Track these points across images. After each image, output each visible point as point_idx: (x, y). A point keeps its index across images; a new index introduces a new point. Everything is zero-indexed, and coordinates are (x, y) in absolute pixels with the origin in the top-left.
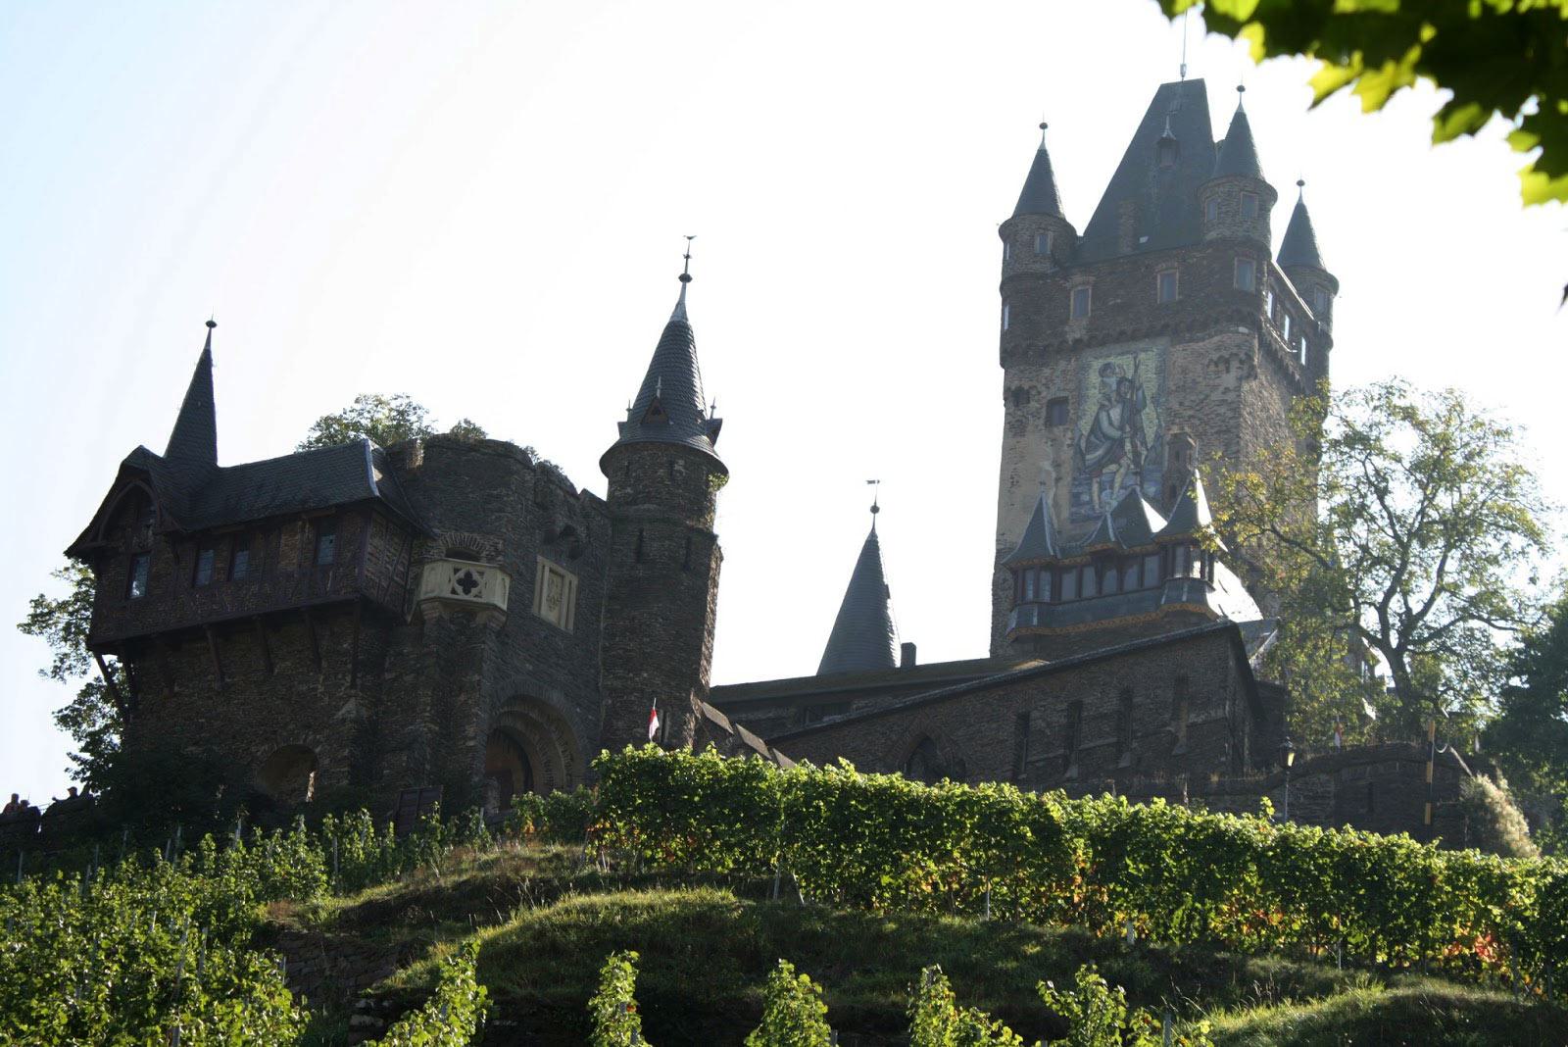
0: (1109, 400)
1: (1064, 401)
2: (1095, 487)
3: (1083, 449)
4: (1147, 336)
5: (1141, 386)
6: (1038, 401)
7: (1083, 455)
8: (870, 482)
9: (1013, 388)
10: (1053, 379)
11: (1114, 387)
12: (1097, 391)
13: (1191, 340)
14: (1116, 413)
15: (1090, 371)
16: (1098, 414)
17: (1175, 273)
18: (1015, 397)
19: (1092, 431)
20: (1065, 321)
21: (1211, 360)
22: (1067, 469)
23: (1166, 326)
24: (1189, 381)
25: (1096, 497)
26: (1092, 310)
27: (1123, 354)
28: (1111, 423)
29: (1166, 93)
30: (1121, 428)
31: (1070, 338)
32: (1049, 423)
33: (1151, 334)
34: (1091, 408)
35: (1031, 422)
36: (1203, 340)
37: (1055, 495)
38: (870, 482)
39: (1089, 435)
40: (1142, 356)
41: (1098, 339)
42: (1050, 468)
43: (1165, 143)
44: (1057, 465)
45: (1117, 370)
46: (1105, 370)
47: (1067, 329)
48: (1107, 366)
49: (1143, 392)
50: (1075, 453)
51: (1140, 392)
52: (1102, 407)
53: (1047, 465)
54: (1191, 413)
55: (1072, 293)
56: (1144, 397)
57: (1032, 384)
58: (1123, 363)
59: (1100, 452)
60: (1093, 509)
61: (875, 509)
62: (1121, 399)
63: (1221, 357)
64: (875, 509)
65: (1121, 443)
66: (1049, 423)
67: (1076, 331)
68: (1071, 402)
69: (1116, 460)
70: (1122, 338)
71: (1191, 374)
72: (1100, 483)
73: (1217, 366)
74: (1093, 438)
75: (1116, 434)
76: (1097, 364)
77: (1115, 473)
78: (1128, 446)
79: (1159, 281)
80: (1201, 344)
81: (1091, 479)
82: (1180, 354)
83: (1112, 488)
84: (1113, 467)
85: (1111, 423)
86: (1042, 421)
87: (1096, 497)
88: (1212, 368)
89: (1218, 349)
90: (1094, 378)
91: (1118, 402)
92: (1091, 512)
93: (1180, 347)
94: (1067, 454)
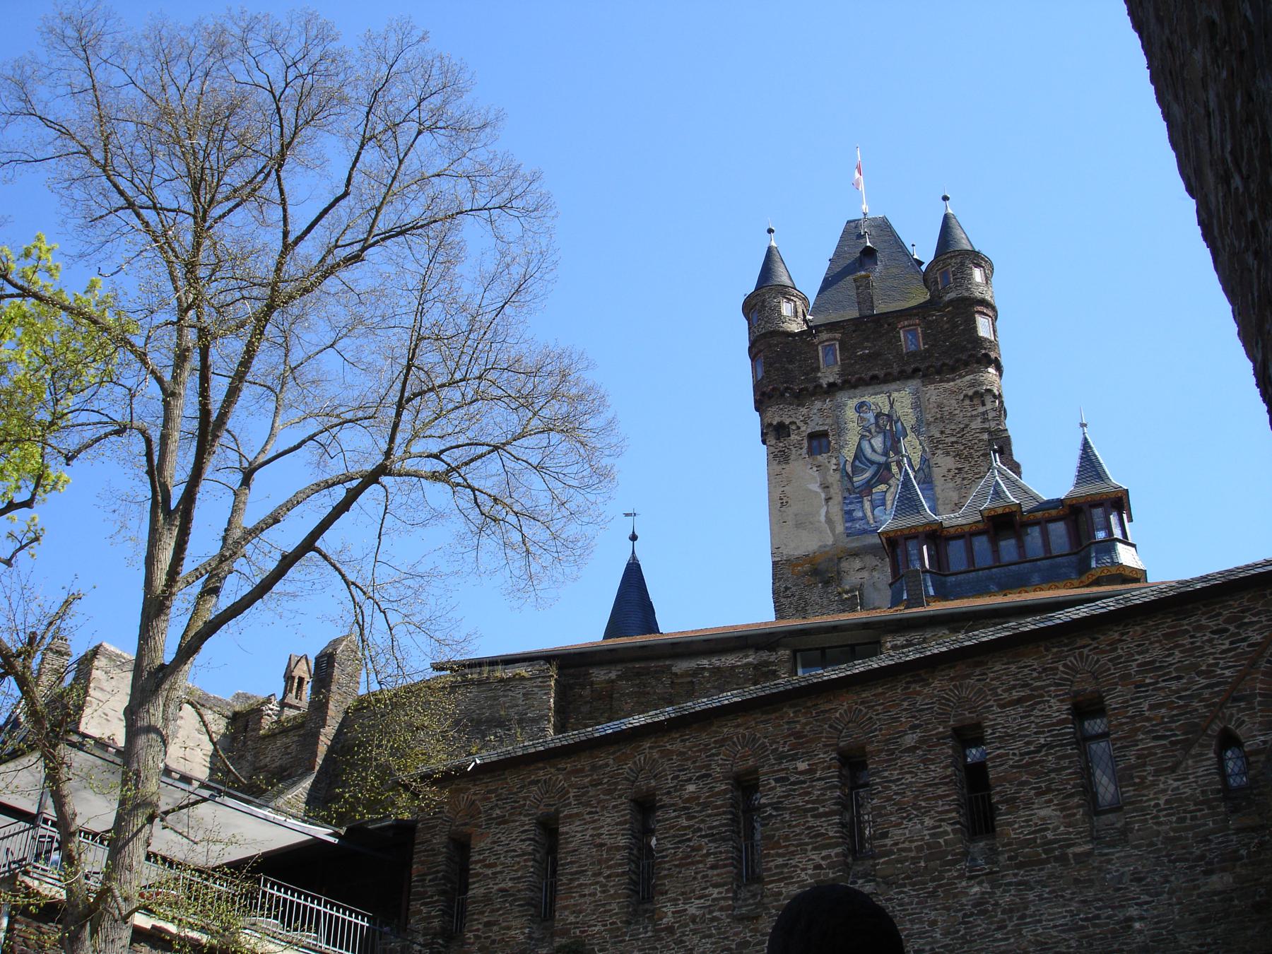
0: (870, 431)
1: (824, 434)
2: (867, 505)
3: (850, 473)
4: (895, 379)
5: (899, 419)
6: (798, 434)
7: (850, 479)
8: (627, 515)
9: (775, 423)
10: (812, 416)
11: (873, 420)
12: (855, 424)
13: (941, 381)
14: (878, 442)
15: (847, 408)
16: (859, 443)
17: (916, 329)
18: (774, 433)
19: (856, 457)
20: (818, 369)
21: (966, 396)
22: (836, 491)
23: (916, 370)
24: (946, 413)
25: (869, 514)
26: (841, 360)
27: (876, 394)
28: (874, 450)
29: (853, 230)
30: (886, 454)
31: (824, 382)
32: (812, 452)
33: (904, 376)
34: (852, 438)
35: (794, 452)
36: (953, 380)
37: (827, 512)
38: (627, 515)
39: (854, 461)
40: (895, 395)
41: (850, 382)
42: (819, 490)
43: (869, 253)
44: (826, 487)
45: (873, 407)
46: (860, 407)
47: (819, 374)
48: (862, 404)
49: (902, 424)
50: (842, 477)
51: (899, 424)
52: (863, 437)
53: (815, 487)
54: (954, 439)
55: (820, 348)
56: (904, 428)
57: (790, 420)
58: (878, 400)
59: (867, 475)
60: (868, 523)
61: (634, 538)
62: (881, 430)
63: (976, 393)
64: (634, 538)
65: (887, 466)
66: (812, 452)
67: (828, 375)
68: (831, 434)
69: (885, 481)
70: (874, 380)
71: (946, 409)
72: (871, 501)
73: (971, 401)
74: (857, 463)
75: (882, 459)
76: (853, 403)
77: (886, 492)
78: (895, 469)
79: (902, 335)
80: (952, 383)
81: (862, 497)
82: (933, 393)
83: (884, 504)
84: (883, 487)
85: (874, 450)
86: (804, 451)
87: (869, 514)
88: (967, 402)
89: (972, 385)
90: (850, 414)
91: (879, 433)
92: (866, 527)
93: (932, 387)
94: (834, 478)
